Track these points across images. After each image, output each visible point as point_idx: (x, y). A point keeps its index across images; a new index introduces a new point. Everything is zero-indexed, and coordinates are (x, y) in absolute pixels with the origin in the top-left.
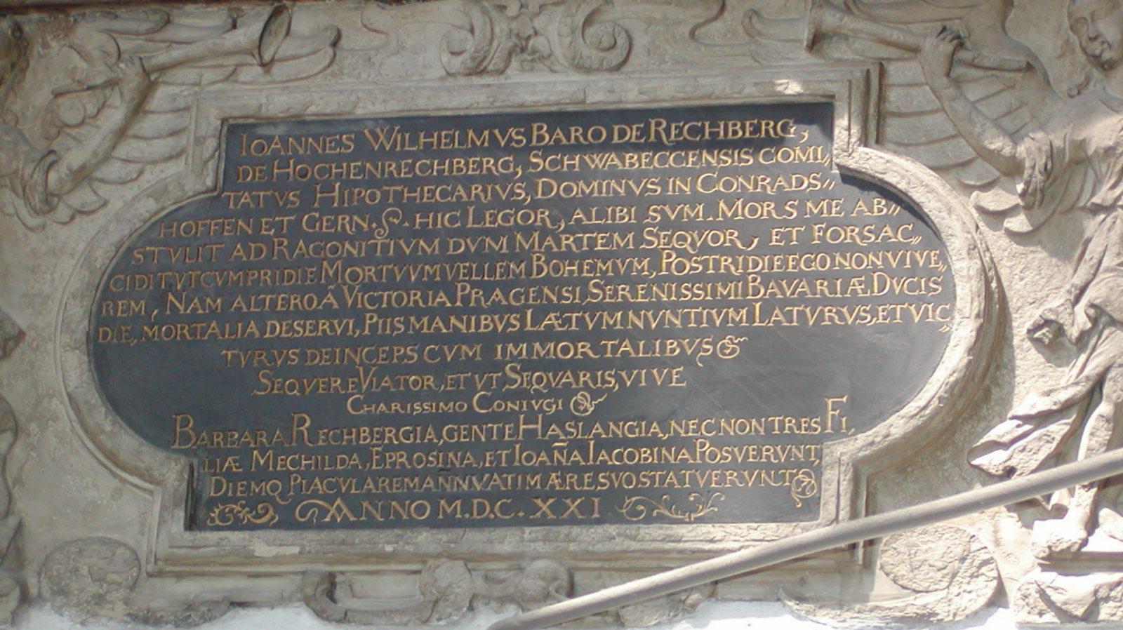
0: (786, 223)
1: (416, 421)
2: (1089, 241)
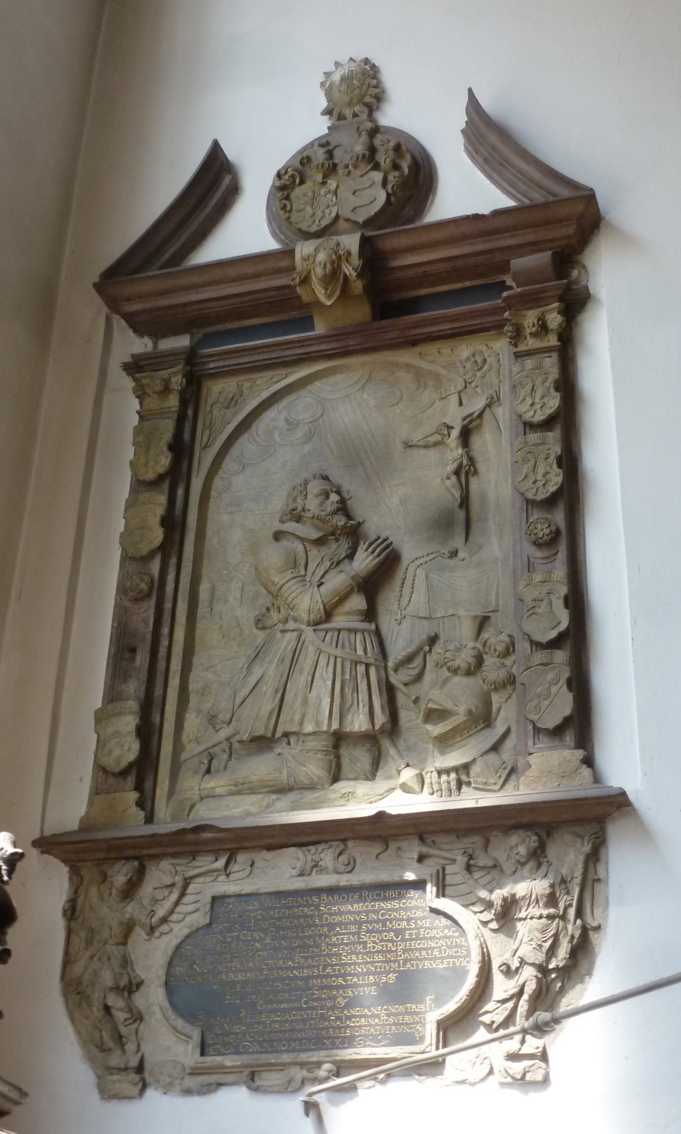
0: (410, 929)
1: (282, 1011)
2: (518, 932)
